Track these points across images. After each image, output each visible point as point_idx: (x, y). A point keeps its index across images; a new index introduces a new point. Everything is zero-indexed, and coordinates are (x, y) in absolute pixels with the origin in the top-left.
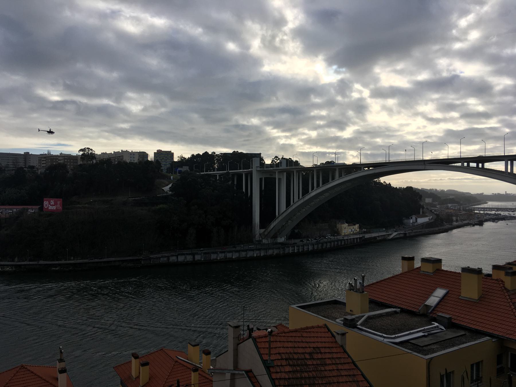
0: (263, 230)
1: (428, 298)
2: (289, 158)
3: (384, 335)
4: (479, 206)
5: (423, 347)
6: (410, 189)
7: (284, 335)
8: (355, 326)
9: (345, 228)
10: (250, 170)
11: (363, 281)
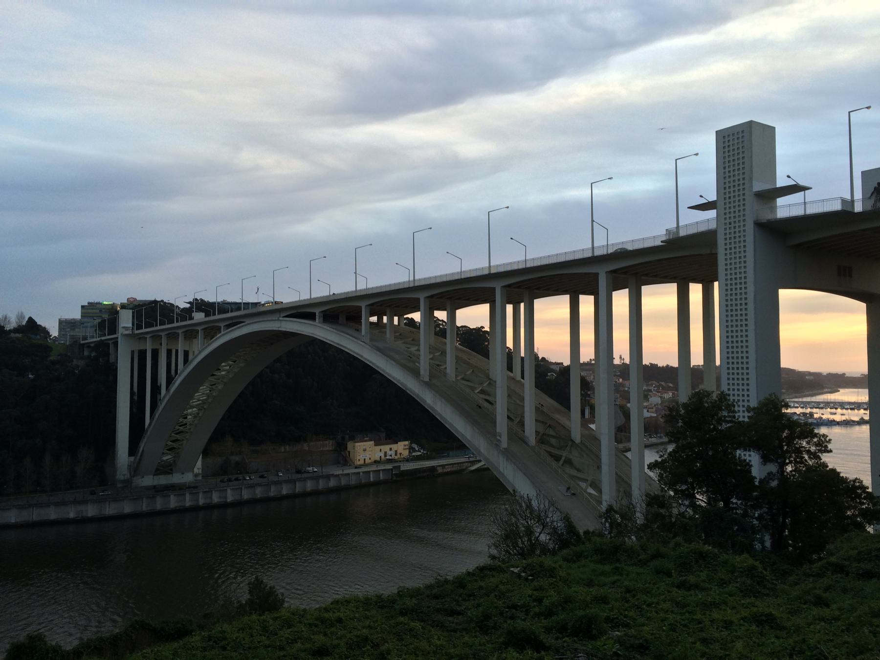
4: (800, 400)
9: (365, 450)
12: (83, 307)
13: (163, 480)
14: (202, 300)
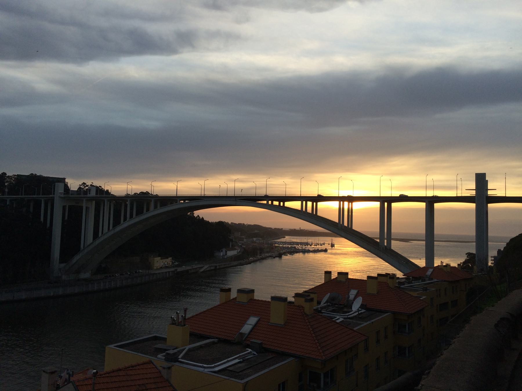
0: (63, 265)
1: (242, 326)
2: (100, 186)
3: (204, 365)
4: (279, 240)
5: (239, 372)
6: (221, 224)
7: (131, 368)
8: (176, 360)
9: (158, 261)
10: (51, 196)
11: (185, 314)
14: (36, 174)
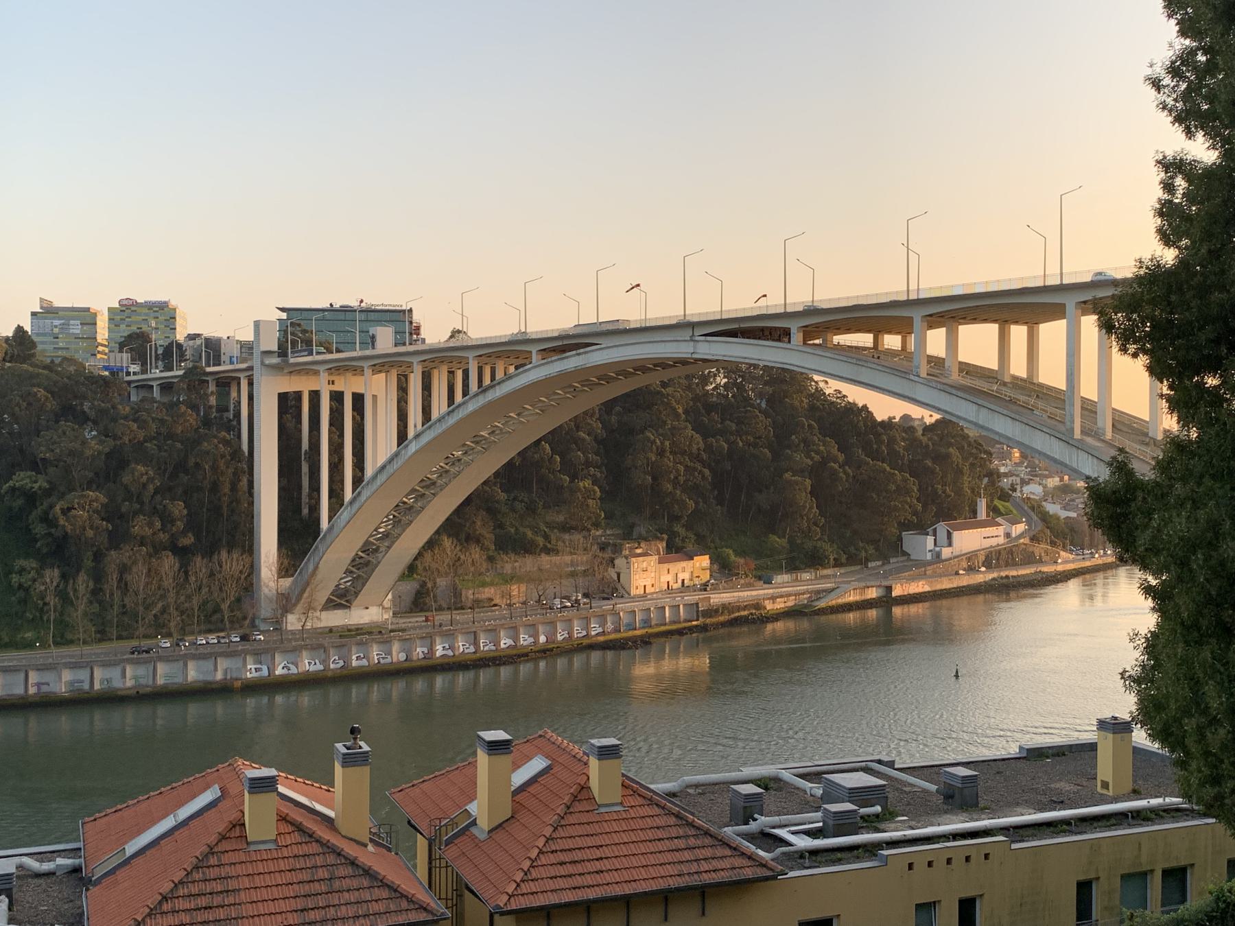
0: (287, 582)
12: (34, 314)
13: (335, 619)
